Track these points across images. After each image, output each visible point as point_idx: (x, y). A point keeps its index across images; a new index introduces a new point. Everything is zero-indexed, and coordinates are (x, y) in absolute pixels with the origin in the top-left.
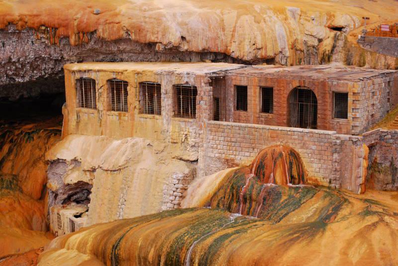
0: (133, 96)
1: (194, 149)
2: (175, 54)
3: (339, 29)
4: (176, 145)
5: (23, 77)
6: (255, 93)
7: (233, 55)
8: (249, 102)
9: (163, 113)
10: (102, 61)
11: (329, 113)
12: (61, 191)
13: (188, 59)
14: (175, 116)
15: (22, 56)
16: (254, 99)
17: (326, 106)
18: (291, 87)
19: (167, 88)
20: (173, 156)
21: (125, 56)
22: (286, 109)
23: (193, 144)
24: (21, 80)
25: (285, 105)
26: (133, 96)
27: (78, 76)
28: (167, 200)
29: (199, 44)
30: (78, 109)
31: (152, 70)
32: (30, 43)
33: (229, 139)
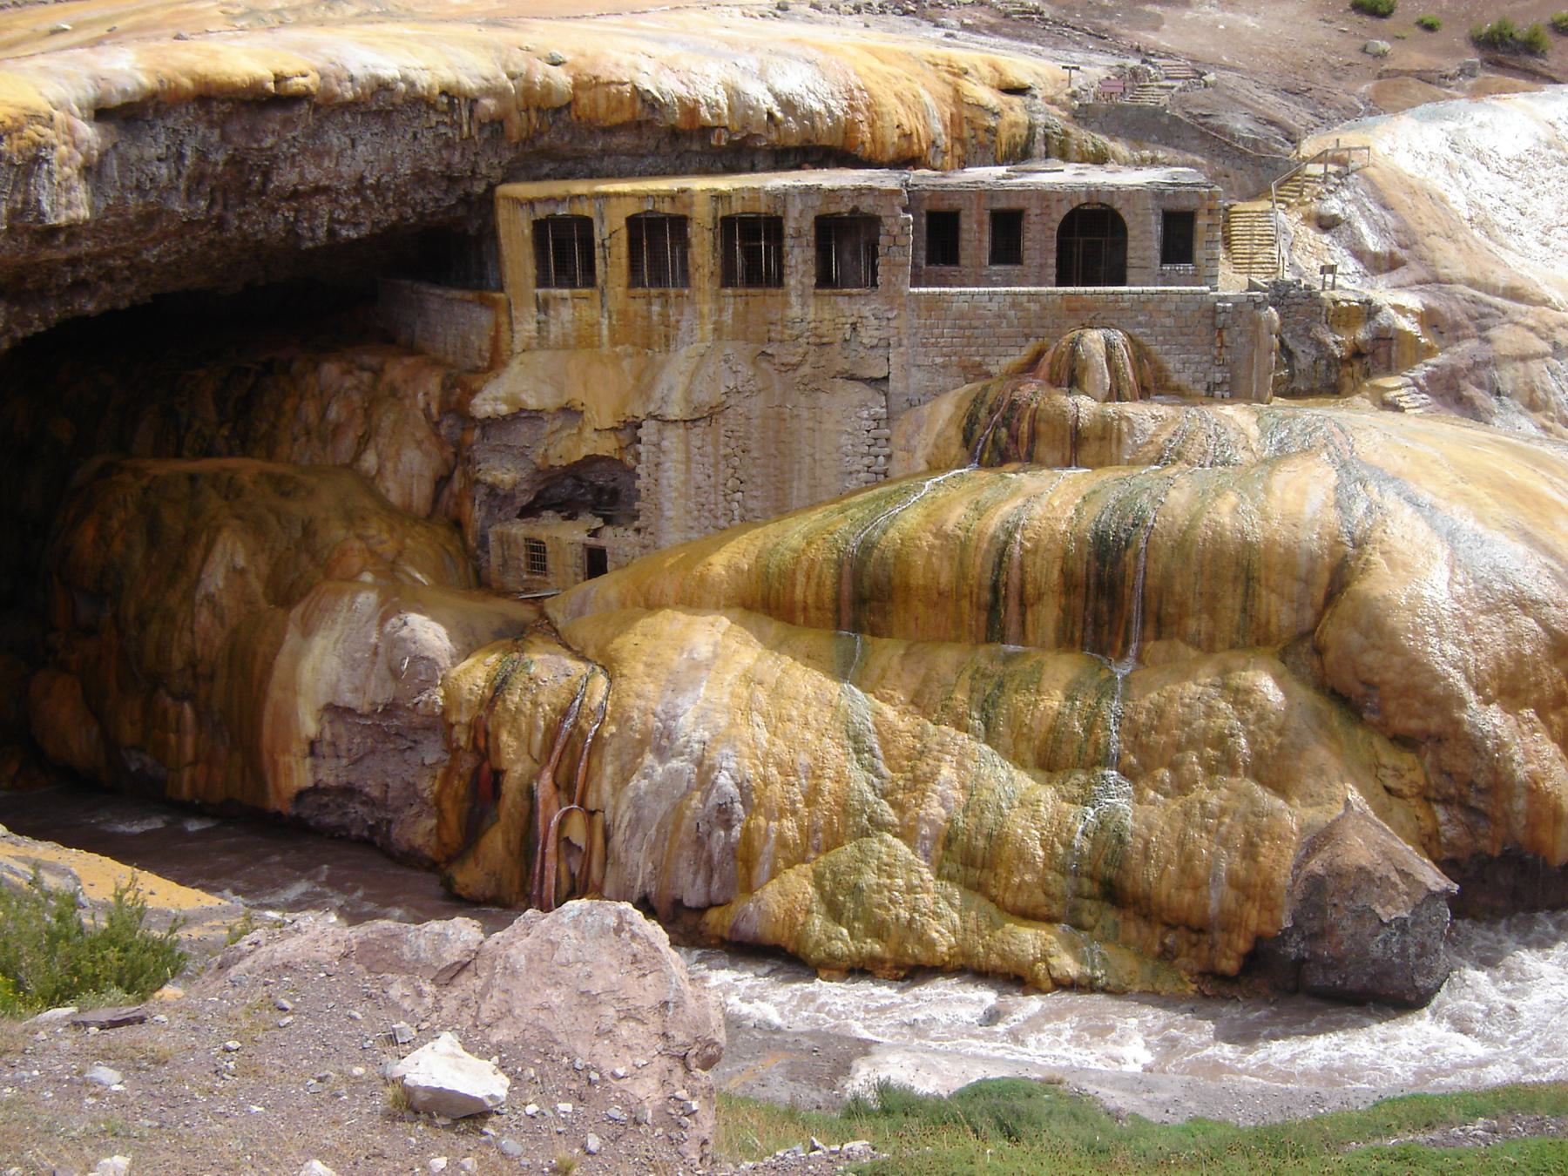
0: (703, 251)
3: (1020, 91)
4: (828, 349)
5: (356, 225)
6: (980, 224)
7: (860, 152)
8: (963, 244)
9: (792, 281)
10: (547, 177)
12: (524, 486)
13: (746, 165)
15: (389, 171)
16: (975, 237)
17: (1145, 239)
18: (1065, 209)
19: (798, 222)
20: (832, 375)
21: (607, 162)
22: (1054, 255)
23: (875, 341)
24: (353, 234)
26: (703, 251)
27: (542, 212)
28: (856, 467)
30: (541, 292)
32: (409, 136)
33: (965, 323)
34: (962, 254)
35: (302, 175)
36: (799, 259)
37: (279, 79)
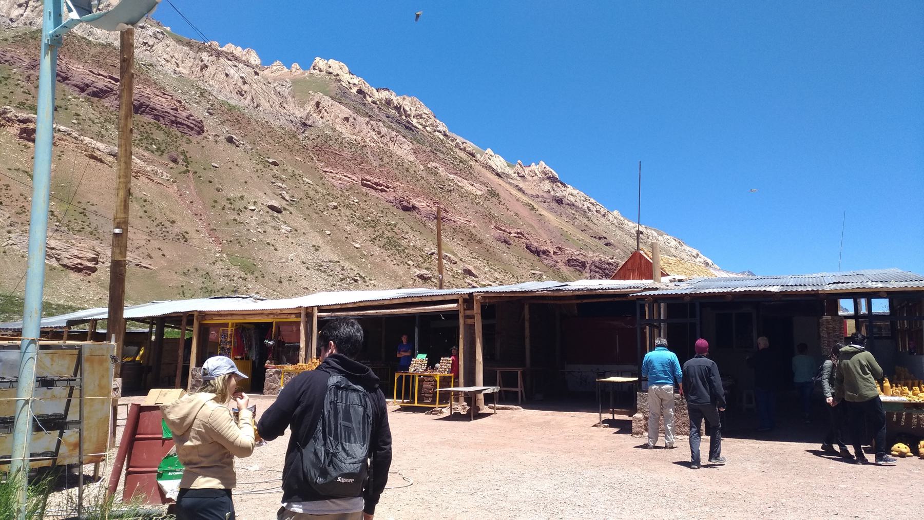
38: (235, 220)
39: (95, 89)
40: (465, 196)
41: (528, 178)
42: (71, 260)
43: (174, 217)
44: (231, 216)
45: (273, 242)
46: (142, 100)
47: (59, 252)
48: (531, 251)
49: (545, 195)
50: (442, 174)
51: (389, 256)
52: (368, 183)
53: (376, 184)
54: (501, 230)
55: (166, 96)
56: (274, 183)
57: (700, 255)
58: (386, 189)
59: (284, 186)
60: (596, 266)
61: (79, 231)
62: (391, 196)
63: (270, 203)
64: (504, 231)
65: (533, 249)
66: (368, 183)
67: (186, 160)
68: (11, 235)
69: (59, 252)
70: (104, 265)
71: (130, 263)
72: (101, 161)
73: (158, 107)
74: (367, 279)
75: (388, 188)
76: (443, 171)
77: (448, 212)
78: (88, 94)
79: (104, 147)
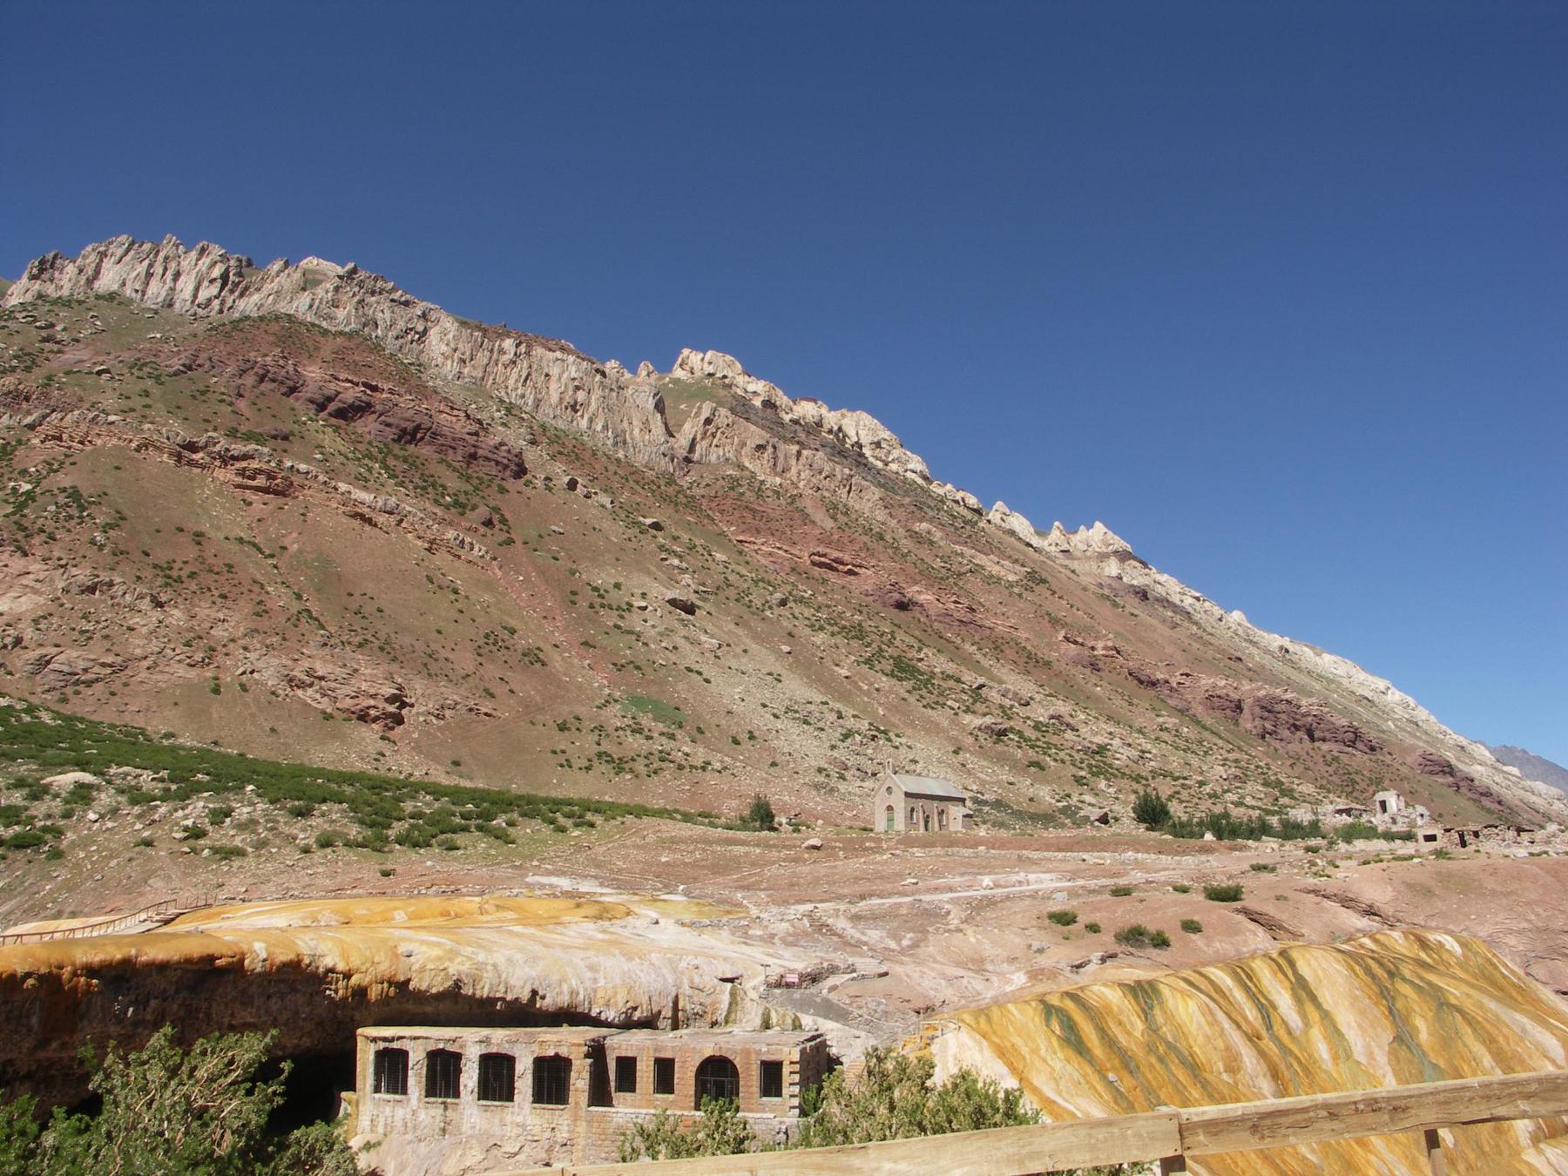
0: (470, 1077)
1: (564, 1148)
2: (524, 1014)
6: (648, 1066)
8: (638, 1079)
11: (756, 1089)
14: (534, 1102)
16: (645, 1074)
25: (693, 1082)
26: (470, 1077)
27: (381, 1045)
29: (551, 1000)
31: (500, 1038)
34: (638, 1086)
35: (232, 1015)
36: (524, 1084)
37: (211, 958)
38: (617, 627)
39: (341, 405)
40: (993, 580)
41: (1077, 554)
42: (356, 701)
43: (513, 623)
44: (610, 619)
45: (695, 667)
46: (418, 419)
47: (333, 685)
48: (1141, 682)
49: (1114, 584)
50: (941, 544)
51: (908, 691)
52: (823, 559)
53: (835, 561)
54: (1075, 643)
55: (456, 412)
56: (666, 559)
57: (1393, 689)
58: (856, 570)
59: (684, 565)
60: (1263, 707)
61: (360, 645)
62: (868, 579)
63: (670, 595)
64: (1082, 645)
65: (1143, 678)
66: (823, 559)
67: (504, 521)
68: (248, 655)
69: (333, 685)
70: (414, 710)
71: (458, 707)
72: (369, 521)
73: (445, 430)
74: (891, 735)
75: (861, 567)
76: (942, 538)
77: (974, 610)
78: (330, 414)
79: (372, 497)
